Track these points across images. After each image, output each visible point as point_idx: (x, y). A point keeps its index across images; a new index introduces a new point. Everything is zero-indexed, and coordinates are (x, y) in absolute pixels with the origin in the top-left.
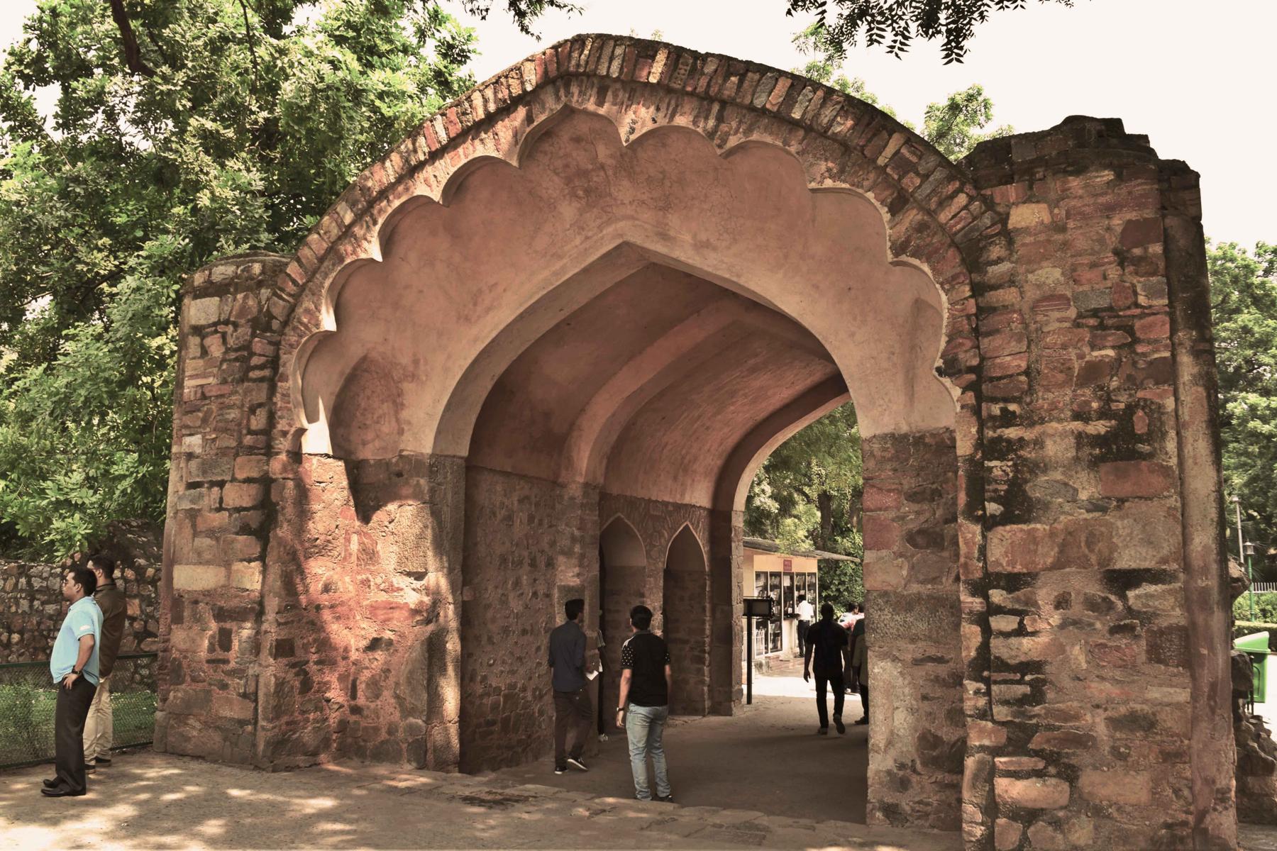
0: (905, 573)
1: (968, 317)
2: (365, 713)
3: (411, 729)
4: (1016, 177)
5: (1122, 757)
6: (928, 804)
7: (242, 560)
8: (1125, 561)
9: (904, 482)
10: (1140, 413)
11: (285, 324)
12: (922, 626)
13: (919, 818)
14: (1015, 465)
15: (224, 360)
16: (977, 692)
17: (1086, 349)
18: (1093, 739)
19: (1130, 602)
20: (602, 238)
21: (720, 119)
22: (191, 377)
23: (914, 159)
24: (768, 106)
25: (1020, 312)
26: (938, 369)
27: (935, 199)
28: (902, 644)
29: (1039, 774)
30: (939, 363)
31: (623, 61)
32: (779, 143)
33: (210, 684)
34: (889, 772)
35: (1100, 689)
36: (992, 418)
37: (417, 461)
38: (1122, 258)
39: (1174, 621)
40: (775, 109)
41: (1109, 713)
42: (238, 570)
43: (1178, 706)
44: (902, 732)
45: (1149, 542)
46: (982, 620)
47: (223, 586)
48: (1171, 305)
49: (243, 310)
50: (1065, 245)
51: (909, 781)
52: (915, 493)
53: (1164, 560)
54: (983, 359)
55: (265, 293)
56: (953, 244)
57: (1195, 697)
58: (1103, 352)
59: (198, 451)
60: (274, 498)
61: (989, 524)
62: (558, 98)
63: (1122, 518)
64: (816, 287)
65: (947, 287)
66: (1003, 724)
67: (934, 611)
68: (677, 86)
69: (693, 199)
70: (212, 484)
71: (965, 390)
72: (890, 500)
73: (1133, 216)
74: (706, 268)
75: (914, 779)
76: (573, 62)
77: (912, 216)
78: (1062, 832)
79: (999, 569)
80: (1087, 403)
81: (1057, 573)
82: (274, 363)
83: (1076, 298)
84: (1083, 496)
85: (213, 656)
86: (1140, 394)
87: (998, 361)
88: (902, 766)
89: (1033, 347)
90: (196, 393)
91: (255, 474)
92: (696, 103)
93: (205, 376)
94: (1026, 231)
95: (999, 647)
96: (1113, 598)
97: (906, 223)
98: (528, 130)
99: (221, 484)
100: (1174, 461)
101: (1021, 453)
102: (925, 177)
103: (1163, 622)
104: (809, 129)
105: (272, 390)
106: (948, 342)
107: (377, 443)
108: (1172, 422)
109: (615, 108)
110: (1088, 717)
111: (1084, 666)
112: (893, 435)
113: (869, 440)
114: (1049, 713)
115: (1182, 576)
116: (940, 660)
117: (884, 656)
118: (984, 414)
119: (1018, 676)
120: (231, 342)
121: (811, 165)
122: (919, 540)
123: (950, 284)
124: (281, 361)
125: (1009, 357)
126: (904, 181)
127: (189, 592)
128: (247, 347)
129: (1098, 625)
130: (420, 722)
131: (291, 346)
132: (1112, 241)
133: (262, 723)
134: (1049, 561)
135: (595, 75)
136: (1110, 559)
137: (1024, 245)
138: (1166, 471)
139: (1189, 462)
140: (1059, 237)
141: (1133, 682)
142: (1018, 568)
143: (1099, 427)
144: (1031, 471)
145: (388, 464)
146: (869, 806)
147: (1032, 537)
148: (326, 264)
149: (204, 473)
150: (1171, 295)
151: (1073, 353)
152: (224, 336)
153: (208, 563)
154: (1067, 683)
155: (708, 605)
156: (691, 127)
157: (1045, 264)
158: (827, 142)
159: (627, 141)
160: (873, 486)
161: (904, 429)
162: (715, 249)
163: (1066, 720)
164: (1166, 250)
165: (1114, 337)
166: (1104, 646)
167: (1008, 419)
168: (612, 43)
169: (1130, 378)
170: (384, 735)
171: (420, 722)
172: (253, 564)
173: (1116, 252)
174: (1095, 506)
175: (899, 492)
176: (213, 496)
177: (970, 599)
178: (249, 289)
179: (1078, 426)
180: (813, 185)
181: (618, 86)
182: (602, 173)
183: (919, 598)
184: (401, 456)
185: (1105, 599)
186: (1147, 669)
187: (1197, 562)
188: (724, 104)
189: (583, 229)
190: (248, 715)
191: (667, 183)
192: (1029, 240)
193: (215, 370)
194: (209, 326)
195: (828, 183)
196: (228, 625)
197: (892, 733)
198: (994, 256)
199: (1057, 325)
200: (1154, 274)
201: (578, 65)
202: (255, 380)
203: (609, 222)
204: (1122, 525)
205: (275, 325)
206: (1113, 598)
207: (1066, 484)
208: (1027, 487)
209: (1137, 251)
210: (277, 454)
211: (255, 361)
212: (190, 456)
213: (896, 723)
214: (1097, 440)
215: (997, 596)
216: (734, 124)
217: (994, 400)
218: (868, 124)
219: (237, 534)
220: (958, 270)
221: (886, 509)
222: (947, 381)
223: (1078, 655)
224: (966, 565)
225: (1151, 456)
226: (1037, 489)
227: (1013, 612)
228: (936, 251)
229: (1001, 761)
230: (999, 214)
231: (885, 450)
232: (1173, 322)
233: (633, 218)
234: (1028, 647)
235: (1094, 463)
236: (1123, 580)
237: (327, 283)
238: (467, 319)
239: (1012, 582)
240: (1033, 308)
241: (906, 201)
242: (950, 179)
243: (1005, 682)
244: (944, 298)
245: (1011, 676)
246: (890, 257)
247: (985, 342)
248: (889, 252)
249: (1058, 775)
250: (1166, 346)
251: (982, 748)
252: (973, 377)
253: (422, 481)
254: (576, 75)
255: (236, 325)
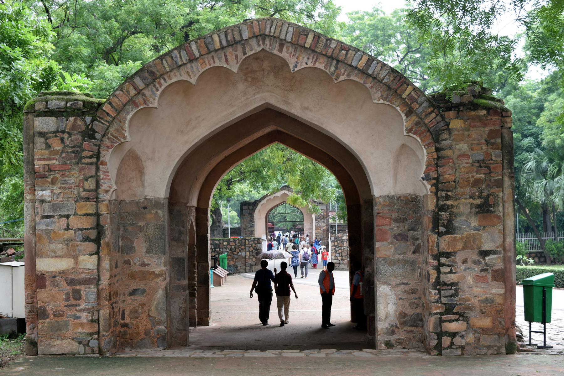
0: (392, 250)
1: (434, 159)
2: (130, 326)
3: (158, 331)
4: (453, 109)
5: (483, 313)
6: (402, 339)
7: (85, 255)
8: (485, 247)
9: (393, 214)
10: (491, 197)
11: (104, 136)
12: (399, 271)
13: (399, 345)
14: (450, 214)
15: (63, 152)
16: (435, 294)
17: (475, 174)
18: (473, 307)
19: (487, 261)
20: (255, 99)
21: (336, 68)
22: (40, 160)
23: (416, 97)
24: (358, 66)
25: (452, 159)
26: (423, 178)
27: (424, 114)
28: (392, 278)
29: (457, 320)
30: (423, 175)
31: (293, 34)
32: (362, 82)
33: (67, 318)
34: (387, 329)
35: (477, 290)
36: (442, 197)
37: (155, 201)
38: (487, 143)
39: (500, 267)
40: (361, 68)
41: (479, 298)
42: (83, 260)
43: (500, 295)
44: (391, 313)
45: (493, 241)
46: (437, 269)
47: (73, 268)
48: (502, 160)
49: (74, 127)
50: (469, 136)
51: (394, 331)
52: (397, 219)
53: (497, 247)
54: (439, 175)
55: (88, 119)
56: (429, 131)
57: (506, 292)
58: (481, 176)
59: (48, 199)
60: (102, 222)
61: (440, 234)
62: (259, 45)
63: (485, 233)
64: (357, 132)
65: (426, 147)
66: (445, 304)
67: (404, 265)
68: (318, 50)
69: (305, 89)
70: (61, 216)
71: (432, 186)
72: (387, 222)
73: (492, 128)
74: (307, 119)
75: (396, 330)
76: (268, 30)
77: (414, 119)
78: (464, 339)
79: (444, 251)
80: (474, 193)
81: (463, 252)
82: (98, 156)
83: (472, 156)
84: (472, 225)
85: (69, 303)
86: (492, 191)
87: (445, 176)
88: (392, 326)
89: (457, 172)
90: (44, 168)
91: (91, 211)
92: (326, 59)
93: (49, 159)
94: (456, 130)
95: (443, 278)
96: (481, 260)
97: (411, 122)
98: (244, 57)
99: (68, 217)
100: (501, 214)
101: (452, 210)
102: (420, 105)
103: (497, 268)
104: (375, 78)
105: (97, 169)
106: (426, 168)
107: (130, 192)
108: (501, 201)
109: (288, 55)
110: (473, 300)
111: (472, 283)
112: (388, 196)
113: (379, 198)
114: (460, 299)
115: (503, 252)
116: (407, 284)
117: (384, 283)
118: (439, 195)
119: (450, 287)
120: (67, 142)
121: (375, 93)
122: (399, 238)
123: (428, 146)
124: (101, 155)
125: (448, 175)
126: (412, 105)
127: (49, 272)
128: (80, 146)
129: (476, 269)
130: (163, 327)
131: (108, 147)
132: (485, 136)
133: (102, 333)
134: (461, 247)
135: (279, 38)
136: (481, 247)
137: (455, 135)
138: (498, 217)
139: (506, 214)
140: (467, 133)
141: (487, 288)
142: (450, 250)
143: (478, 202)
144: (455, 216)
145: (138, 203)
146: (379, 343)
147: (455, 239)
148: (127, 107)
149: (54, 210)
150: (503, 157)
151: (470, 175)
152: (62, 140)
153: (60, 257)
154: (467, 289)
155: (196, 263)
156: (323, 69)
157: (461, 142)
158: (382, 85)
159: (293, 70)
160: (380, 216)
161: (393, 194)
162: (311, 111)
163: (465, 301)
164: (502, 141)
165: (485, 170)
166: (478, 276)
167: (448, 198)
168: (287, 25)
169: (488, 185)
170: (142, 336)
171: (163, 327)
172: (93, 256)
173: (486, 141)
174: (476, 229)
175: (390, 218)
176: (61, 223)
177: (433, 261)
178: (77, 115)
179: (471, 201)
180: (376, 101)
181: (289, 45)
182: (262, 72)
183: (398, 261)
184: (146, 199)
185: (478, 260)
186: (491, 283)
187: (507, 248)
188: (338, 61)
189: (246, 95)
190: (96, 330)
191: (294, 81)
192: (456, 133)
193: (57, 157)
194: (51, 133)
195: (381, 101)
196: (78, 287)
197: (387, 313)
198: (444, 138)
199: (465, 165)
200: (498, 149)
201: (270, 32)
202: (86, 164)
203: (258, 93)
204: (485, 235)
205: (98, 136)
206: (481, 260)
207: (467, 221)
208: (453, 222)
209: (493, 141)
210: (102, 201)
211: (85, 154)
212: (43, 201)
213: (389, 309)
214: (478, 206)
215: (443, 260)
216: (342, 71)
217: (443, 191)
218: (399, 80)
219: (81, 241)
220: (431, 141)
221: (386, 225)
222: (425, 182)
223: (470, 280)
224: (431, 249)
225: (495, 212)
226: (458, 222)
227: (448, 266)
228: (423, 133)
229: (444, 317)
230: (446, 122)
231: (385, 202)
232: (503, 166)
233: (271, 92)
234: (453, 278)
235: (476, 214)
236: (485, 254)
237: (129, 117)
238: (182, 132)
239: (448, 255)
240: (458, 157)
241: (412, 113)
242: (429, 107)
243: (446, 290)
244: (425, 151)
245: (448, 287)
246: (405, 133)
247: (440, 170)
248: (405, 132)
249: (463, 320)
250: (500, 175)
251: (437, 313)
252: (435, 181)
253: (159, 212)
254: (269, 36)
255: (70, 134)
